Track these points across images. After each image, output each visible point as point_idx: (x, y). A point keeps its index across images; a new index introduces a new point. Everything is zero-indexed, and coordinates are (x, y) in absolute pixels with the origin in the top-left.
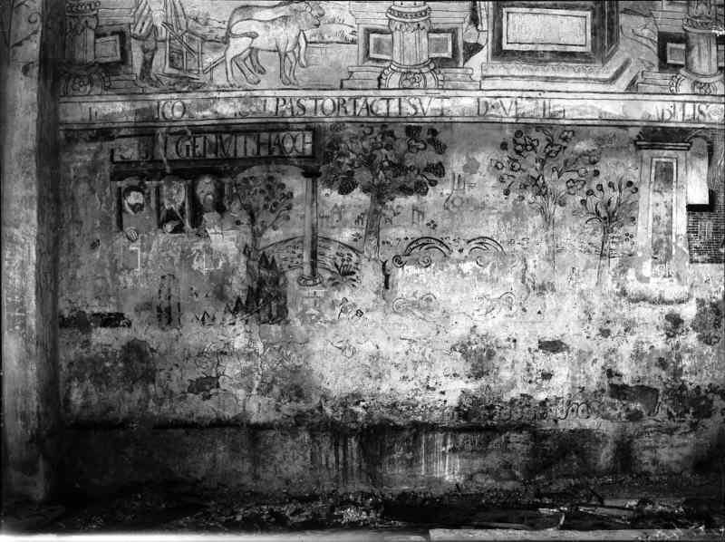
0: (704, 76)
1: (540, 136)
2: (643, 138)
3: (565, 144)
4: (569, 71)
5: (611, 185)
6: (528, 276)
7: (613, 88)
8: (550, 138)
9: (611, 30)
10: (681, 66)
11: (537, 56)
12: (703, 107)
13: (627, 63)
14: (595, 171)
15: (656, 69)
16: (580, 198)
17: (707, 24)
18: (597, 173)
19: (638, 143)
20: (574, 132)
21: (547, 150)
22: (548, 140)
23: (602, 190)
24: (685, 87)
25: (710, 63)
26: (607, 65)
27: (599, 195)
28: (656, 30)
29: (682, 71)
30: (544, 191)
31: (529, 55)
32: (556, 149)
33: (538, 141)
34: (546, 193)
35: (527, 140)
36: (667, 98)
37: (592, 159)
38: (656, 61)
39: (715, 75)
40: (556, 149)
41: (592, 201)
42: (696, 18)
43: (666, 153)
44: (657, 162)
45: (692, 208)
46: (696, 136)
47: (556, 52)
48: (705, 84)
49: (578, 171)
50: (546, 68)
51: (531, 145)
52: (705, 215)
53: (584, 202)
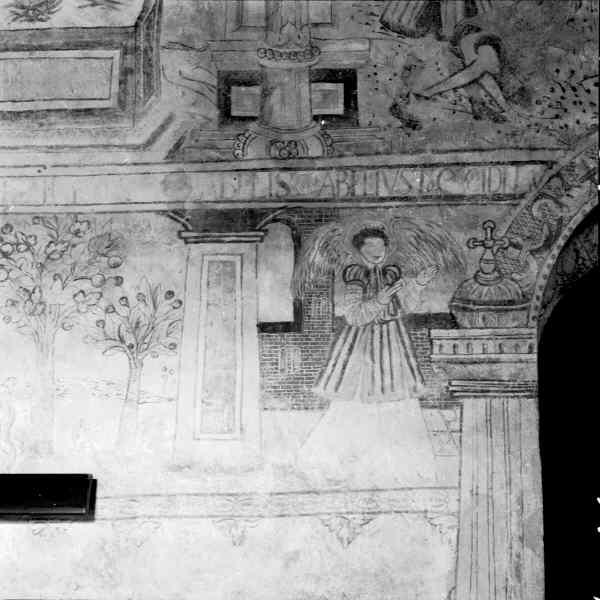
0: (290, 130)
1: (41, 232)
2: (190, 227)
3: (76, 240)
4: (84, 133)
5: (141, 297)
6: (13, 430)
7: (147, 156)
8: (54, 233)
9: (148, 75)
10: (253, 119)
11: (37, 118)
12: (285, 177)
13: (170, 119)
14: (117, 278)
15: (213, 126)
16: (96, 318)
17: (296, 53)
18: (119, 281)
19: (184, 234)
20: (89, 223)
21: (49, 251)
22: (52, 236)
23: (127, 305)
24: (253, 152)
25: (299, 111)
26: (141, 125)
27: (124, 311)
28: (214, 70)
29: (253, 126)
30: (40, 308)
31: (27, 117)
32: (60, 247)
33: (36, 238)
34: (44, 310)
35: (19, 235)
36: (229, 166)
37: (113, 260)
38: (214, 113)
39: (307, 128)
40: (60, 247)
41: (113, 322)
42: (280, 46)
43: (225, 248)
44: (211, 262)
45: (264, 328)
46: (275, 220)
47: (66, 110)
48: (290, 142)
49: (90, 279)
50: (49, 134)
51: (26, 243)
52: (289, 336)
53: (101, 323)
